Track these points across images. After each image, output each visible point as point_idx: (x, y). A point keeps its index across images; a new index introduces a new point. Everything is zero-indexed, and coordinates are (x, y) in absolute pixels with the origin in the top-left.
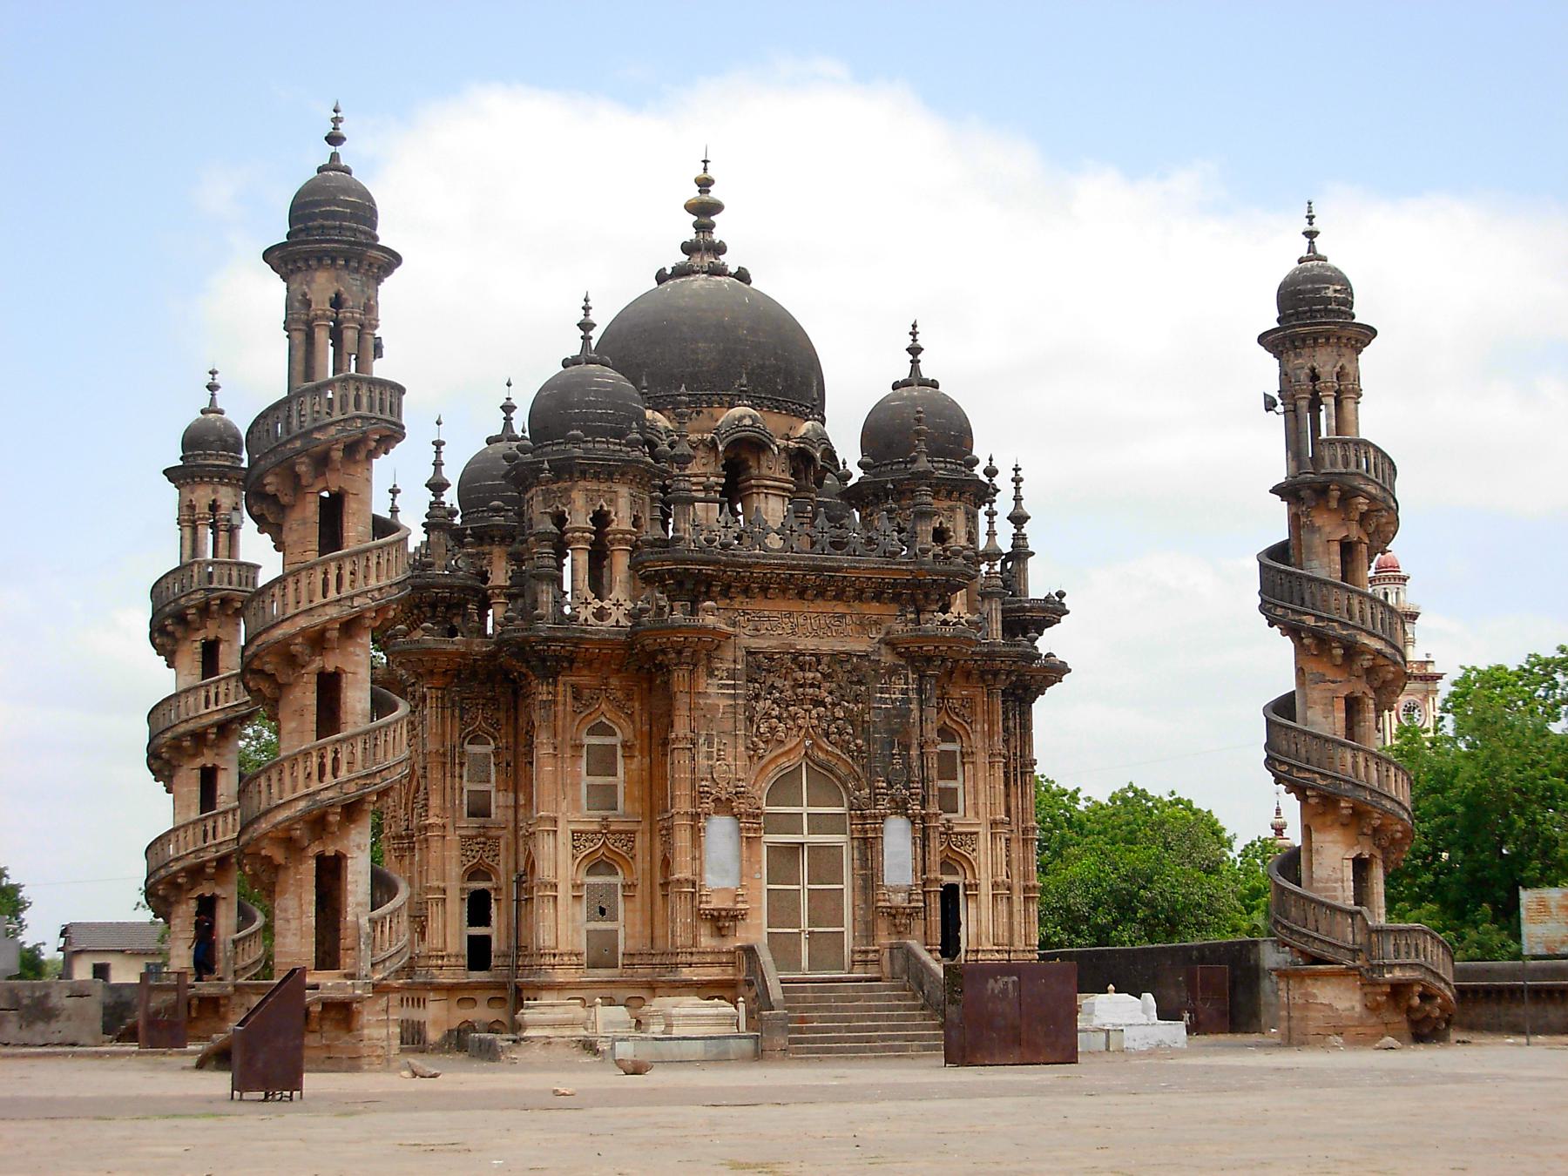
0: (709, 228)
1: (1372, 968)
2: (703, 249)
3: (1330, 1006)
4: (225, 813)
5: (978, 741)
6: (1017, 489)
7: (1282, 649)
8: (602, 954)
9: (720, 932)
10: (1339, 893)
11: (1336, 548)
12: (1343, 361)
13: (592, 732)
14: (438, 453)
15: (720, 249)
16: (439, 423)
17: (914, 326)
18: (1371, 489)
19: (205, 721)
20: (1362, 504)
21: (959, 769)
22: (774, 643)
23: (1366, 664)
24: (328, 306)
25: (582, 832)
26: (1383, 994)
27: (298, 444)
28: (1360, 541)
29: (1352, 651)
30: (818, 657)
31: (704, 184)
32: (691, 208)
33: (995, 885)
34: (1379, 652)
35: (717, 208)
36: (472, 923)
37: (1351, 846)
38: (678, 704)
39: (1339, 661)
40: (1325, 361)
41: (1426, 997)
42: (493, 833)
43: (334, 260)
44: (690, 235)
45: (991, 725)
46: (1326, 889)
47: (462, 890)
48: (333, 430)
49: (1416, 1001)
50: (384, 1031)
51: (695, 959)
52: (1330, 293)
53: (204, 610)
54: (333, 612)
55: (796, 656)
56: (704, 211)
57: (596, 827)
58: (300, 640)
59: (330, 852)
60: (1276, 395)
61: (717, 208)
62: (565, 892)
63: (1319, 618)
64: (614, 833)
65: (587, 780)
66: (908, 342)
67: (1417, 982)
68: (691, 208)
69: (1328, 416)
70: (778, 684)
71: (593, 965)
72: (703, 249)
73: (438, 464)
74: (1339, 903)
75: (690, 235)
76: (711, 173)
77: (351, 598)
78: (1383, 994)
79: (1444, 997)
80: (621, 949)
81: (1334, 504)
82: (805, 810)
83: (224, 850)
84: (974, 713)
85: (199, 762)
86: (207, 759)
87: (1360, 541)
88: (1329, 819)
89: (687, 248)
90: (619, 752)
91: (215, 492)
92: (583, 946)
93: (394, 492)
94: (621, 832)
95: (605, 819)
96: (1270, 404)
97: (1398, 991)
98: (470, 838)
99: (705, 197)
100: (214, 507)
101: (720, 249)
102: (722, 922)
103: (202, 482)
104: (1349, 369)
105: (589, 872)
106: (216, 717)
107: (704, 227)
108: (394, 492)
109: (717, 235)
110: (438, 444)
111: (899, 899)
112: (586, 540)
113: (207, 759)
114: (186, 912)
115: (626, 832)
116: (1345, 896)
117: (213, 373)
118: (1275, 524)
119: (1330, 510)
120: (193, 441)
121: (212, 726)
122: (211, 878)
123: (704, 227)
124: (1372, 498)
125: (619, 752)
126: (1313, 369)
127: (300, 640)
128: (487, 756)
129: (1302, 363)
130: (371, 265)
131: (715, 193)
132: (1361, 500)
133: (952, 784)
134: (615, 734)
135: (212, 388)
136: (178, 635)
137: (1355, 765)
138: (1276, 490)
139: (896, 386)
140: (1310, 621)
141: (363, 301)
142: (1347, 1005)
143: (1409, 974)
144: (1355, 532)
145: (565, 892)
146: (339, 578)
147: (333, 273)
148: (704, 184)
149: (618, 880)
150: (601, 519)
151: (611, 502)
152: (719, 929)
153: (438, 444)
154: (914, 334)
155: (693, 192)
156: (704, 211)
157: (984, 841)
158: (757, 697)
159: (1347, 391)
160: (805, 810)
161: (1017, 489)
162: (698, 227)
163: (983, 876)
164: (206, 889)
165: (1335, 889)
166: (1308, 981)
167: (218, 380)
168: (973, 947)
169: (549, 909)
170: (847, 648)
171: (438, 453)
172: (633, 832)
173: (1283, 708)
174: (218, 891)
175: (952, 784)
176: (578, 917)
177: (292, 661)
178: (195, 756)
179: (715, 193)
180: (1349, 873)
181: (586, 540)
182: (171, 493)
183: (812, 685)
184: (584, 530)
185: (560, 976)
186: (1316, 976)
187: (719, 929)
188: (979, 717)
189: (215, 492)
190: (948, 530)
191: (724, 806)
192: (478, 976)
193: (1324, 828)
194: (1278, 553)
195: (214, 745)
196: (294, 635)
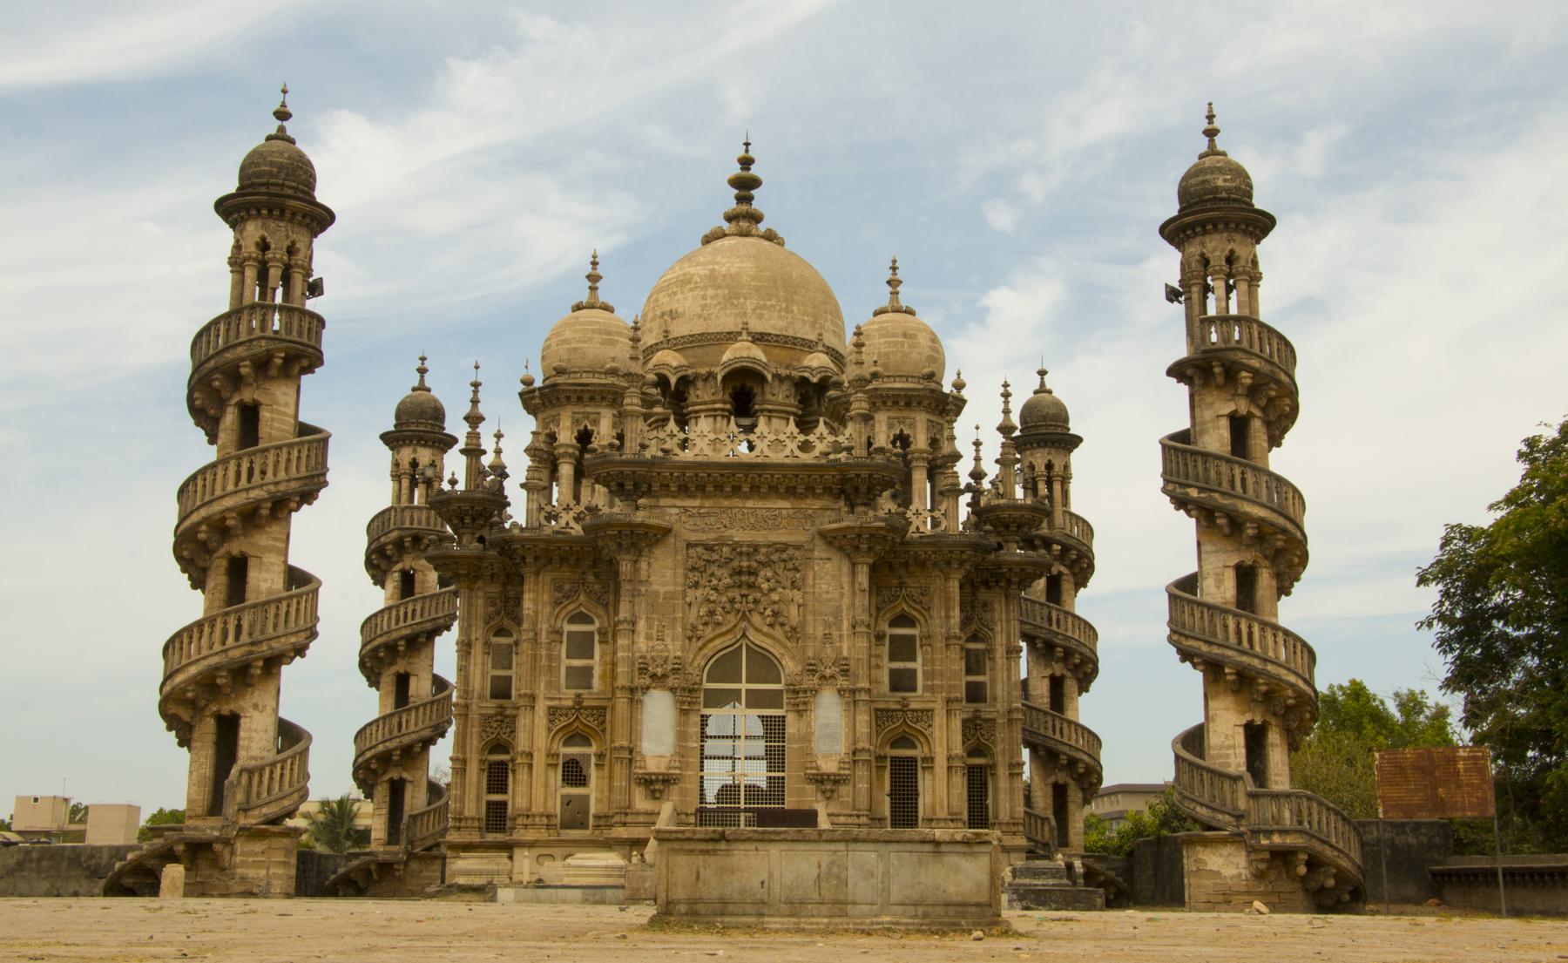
0: (749, 200)
1: (1255, 833)
2: (744, 218)
3: (1218, 873)
4: (417, 708)
5: (937, 626)
6: (1006, 402)
7: (1185, 526)
8: (575, 816)
9: (655, 795)
10: (1232, 760)
11: (1225, 423)
12: (1232, 245)
13: (572, 621)
14: (476, 392)
16: (477, 367)
17: (894, 261)
18: (1255, 363)
19: (394, 635)
20: (1246, 378)
21: (919, 652)
22: (712, 536)
23: (1250, 532)
24: (253, 249)
25: (556, 708)
26: (1262, 860)
27: (212, 363)
28: (1250, 415)
29: (1236, 523)
30: (756, 548)
31: (746, 162)
32: (736, 183)
33: (949, 758)
34: (1263, 520)
35: (755, 183)
36: (490, 791)
37: (1243, 713)
38: (622, 592)
39: (1227, 530)
40: (1215, 246)
41: (1314, 863)
42: (508, 712)
43: (259, 211)
44: (731, 204)
45: (948, 609)
46: (1220, 756)
47: (482, 762)
48: (240, 351)
49: (1302, 870)
50: (263, 872)
51: (629, 819)
52: (1220, 183)
53: (399, 545)
54: (228, 503)
55: (735, 547)
56: (745, 185)
57: (569, 703)
58: (204, 528)
59: (226, 710)
60: (1176, 285)
61: (755, 183)
62: (539, 761)
63: (1201, 490)
64: (586, 708)
65: (566, 662)
66: (888, 275)
67: (1303, 850)
68: (736, 183)
69: (1218, 300)
70: (719, 573)
71: (567, 825)
72: (744, 218)
73: (475, 402)
74: (1232, 770)
76: (752, 154)
77: (247, 490)
78: (1262, 860)
79: (1338, 867)
80: (592, 811)
81: (1220, 380)
82: (744, 686)
83: (406, 740)
84: (931, 600)
85: (394, 669)
86: (401, 666)
87: (1250, 415)
88: (1222, 686)
89: (730, 218)
90: (597, 638)
91: (415, 451)
92: (556, 807)
93: (499, 436)
94: (593, 708)
95: (579, 696)
96: (1172, 295)
97: (1282, 856)
98: (491, 716)
99: (745, 173)
100: (414, 464)
101: (756, 218)
102: (657, 785)
103: (405, 445)
104: (1242, 251)
105: (567, 743)
106: (404, 632)
107: (744, 199)
108: (499, 436)
109: (757, 205)
110: (476, 385)
111: (829, 767)
112: (571, 456)
113: (401, 666)
114: (382, 791)
115: (597, 708)
116: (1236, 761)
117: (423, 359)
118: (1172, 409)
119: (1218, 387)
120: (405, 413)
121: (402, 638)
122: (398, 764)
123: (744, 199)
124: (1255, 372)
125: (597, 638)
126: (1202, 255)
127: (204, 528)
128: (510, 646)
129: (1194, 249)
130: (293, 214)
131: (755, 170)
132: (1244, 374)
133: (910, 665)
134: (591, 622)
135: (422, 371)
136: (383, 566)
137: (1238, 632)
138: (1170, 372)
139: (876, 314)
140: (1194, 493)
141: (287, 243)
142: (1235, 872)
143: (1290, 840)
144: (1243, 407)
145: (539, 761)
146: (238, 474)
147: (260, 222)
148: (746, 162)
149: (592, 750)
150: (584, 437)
151: (596, 422)
152: (653, 792)
153: (476, 385)
154: (894, 269)
155: (736, 170)
156: (745, 185)
157: (939, 719)
158: (696, 585)
159: (1245, 275)
160: (744, 686)
161: (1006, 402)
163: (938, 749)
164: (394, 774)
165: (1228, 756)
166: (1199, 848)
167: (427, 364)
168: (929, 815)
169: (522, 775)
170: (783, 539)
171: (476, 392)
172: (605, 708)
173: (1189, 584)
174: (405, 775)
175: (910, 665)
176: (552, 782)
177: (206, 549)
178: (393, 663)
179: (755, 170)
180: (1240, 739)
181: (571, 456)
182: (385, 454)
183: (750, 573)
184: (567, 446)
185: (530, 835)
186: (1205, 842)
187: (653, 792)
188: (936, 602)
189: (415, 451)
190: (908, 436)
191: (658, 680)
192: (491, 837)
193: (1217, 694)
194: (1183, 437)
195: (405, 655)
196: (199, 524)
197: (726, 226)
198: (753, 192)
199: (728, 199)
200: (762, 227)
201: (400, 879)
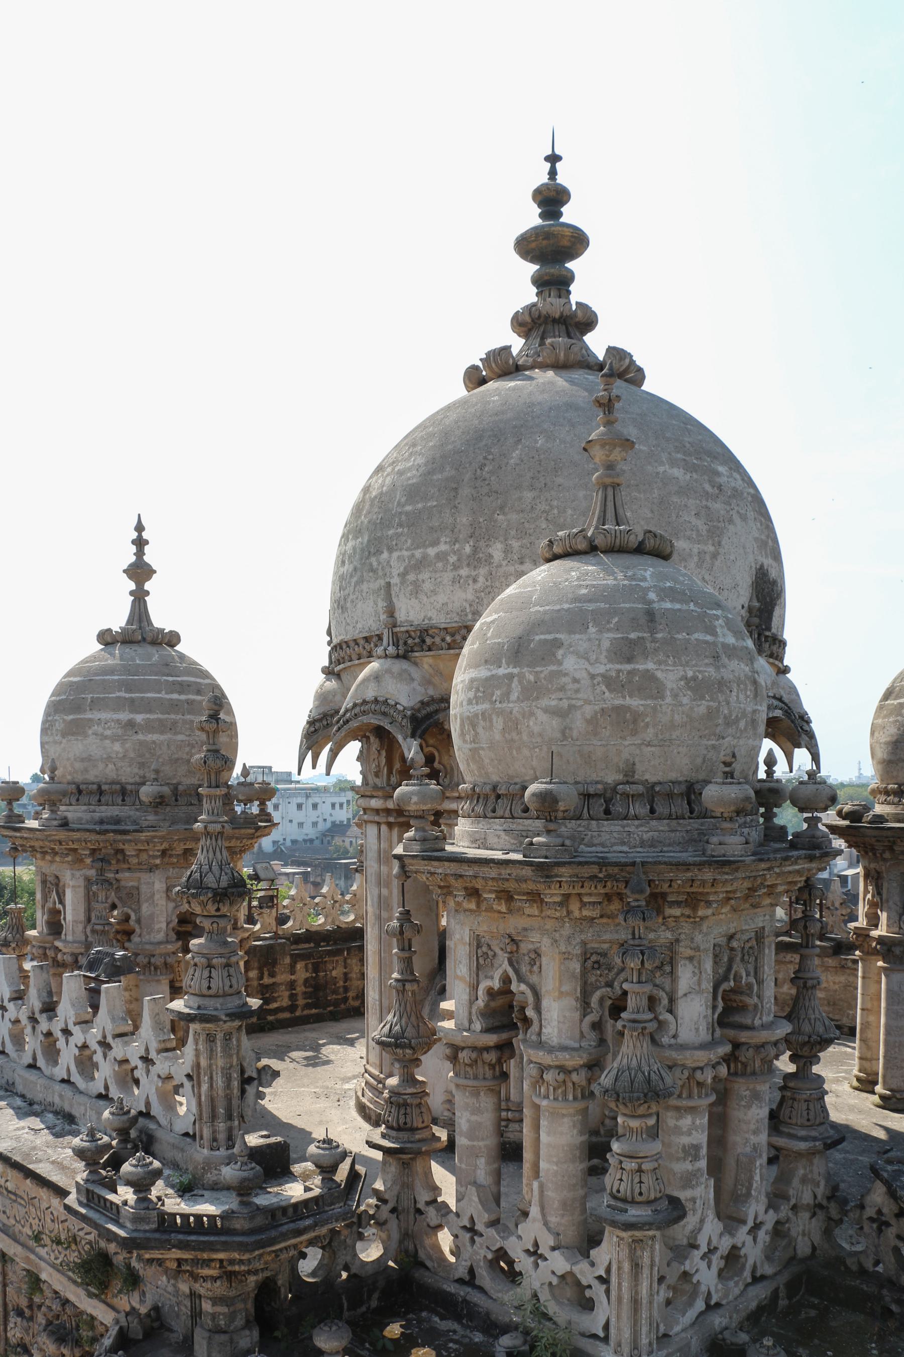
2: (555, 324)
15: (586, 321)
31: (552, 199)
32: (531, 246)
35: (577, 242)
44: (529, 295)
56: (552, 248)
61: (577, 242)
68: (531, 246)
72: (555, 324)
75: (529, 295)
101: (586, 321)
107: (554, 282)
109: (578, 294)
123: (554, 282)
131: (569, 215)
148: (552, 199)
155: (531, 217)
156: (552, 248)
162: (540, 282)
197: (517, 344)
198: (570, 265)
199: (519, 285)
200: (597, 343)
201: (194, 1176)
